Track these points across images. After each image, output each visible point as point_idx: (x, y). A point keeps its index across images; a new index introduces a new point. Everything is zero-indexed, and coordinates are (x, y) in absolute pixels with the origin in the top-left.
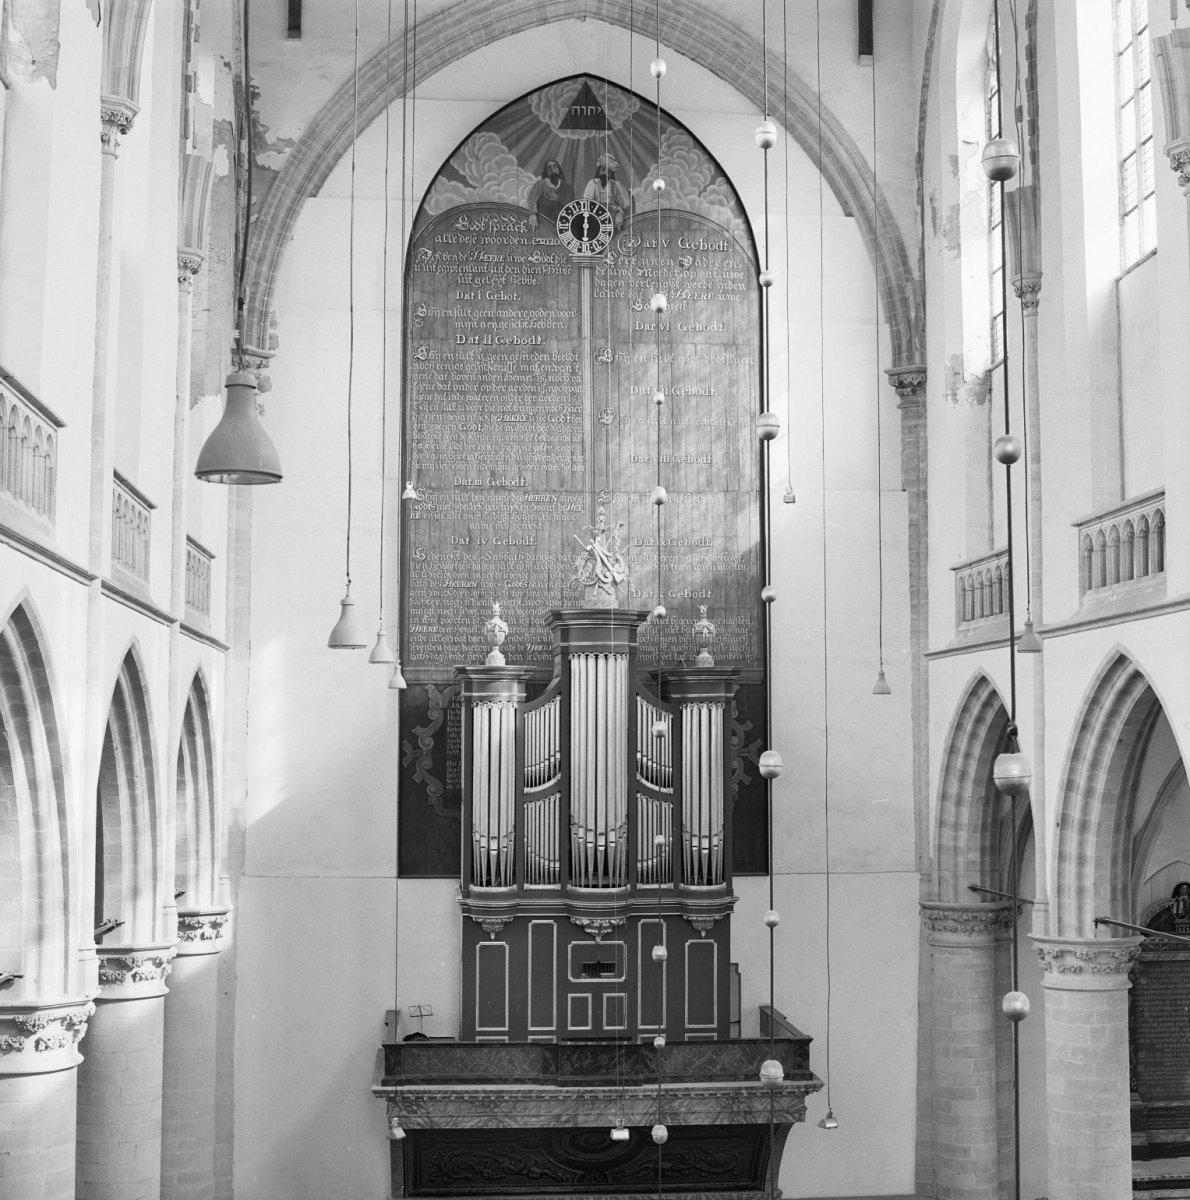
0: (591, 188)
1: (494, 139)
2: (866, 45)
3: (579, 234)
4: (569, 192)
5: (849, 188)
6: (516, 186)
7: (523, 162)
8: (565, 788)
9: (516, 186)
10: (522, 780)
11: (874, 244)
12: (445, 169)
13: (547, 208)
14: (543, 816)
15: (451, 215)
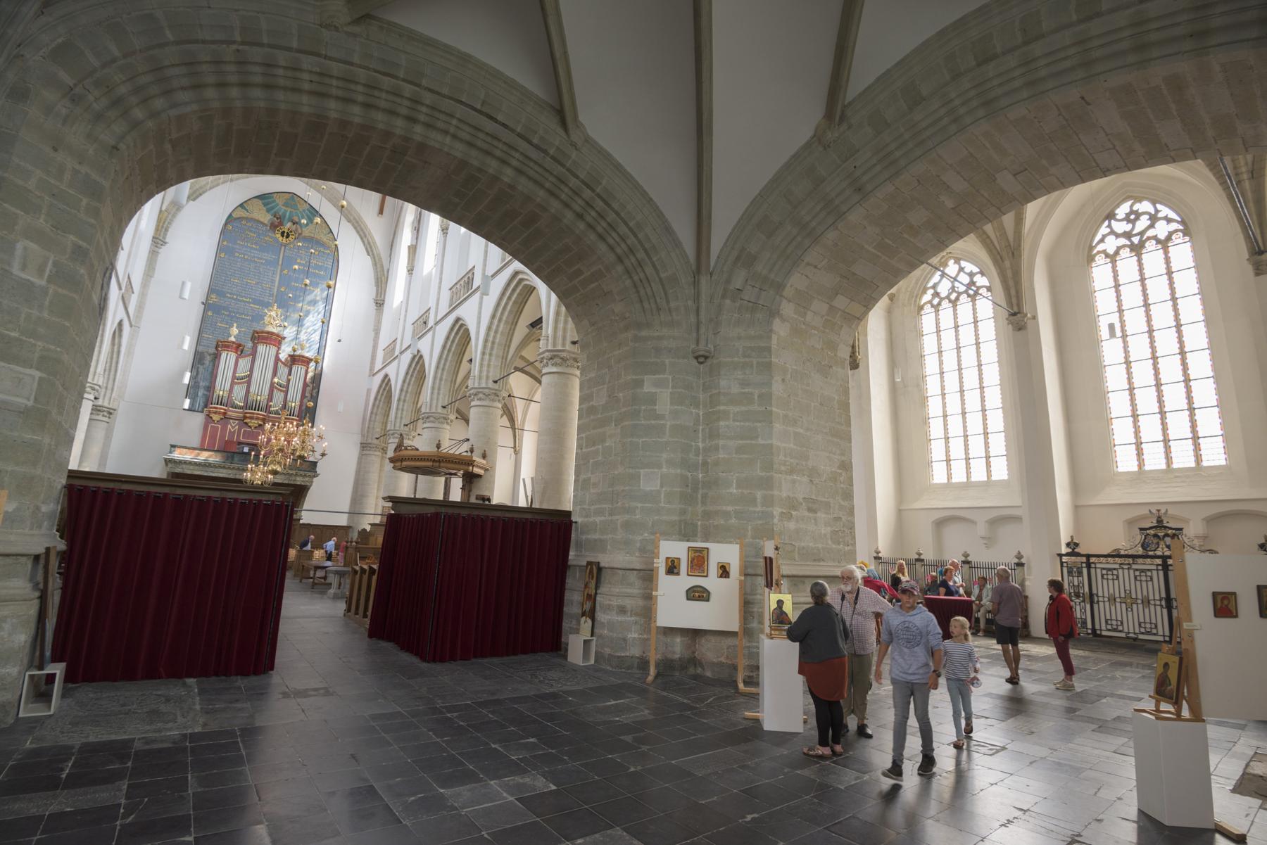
0: (289, 225)
1: (260, 202)
2: (381, 212)
3: (283, 234)
4: (281, 224)
5: (370, 248)
6: (266, 218)
7: (268, 211)
8: (249, 383)
9: (266, 218)
10: (234, 377)
11: (375, 264)
12: (241, 205)
13: (273, 227)
14: (239, 391)
15: (240, 218)
